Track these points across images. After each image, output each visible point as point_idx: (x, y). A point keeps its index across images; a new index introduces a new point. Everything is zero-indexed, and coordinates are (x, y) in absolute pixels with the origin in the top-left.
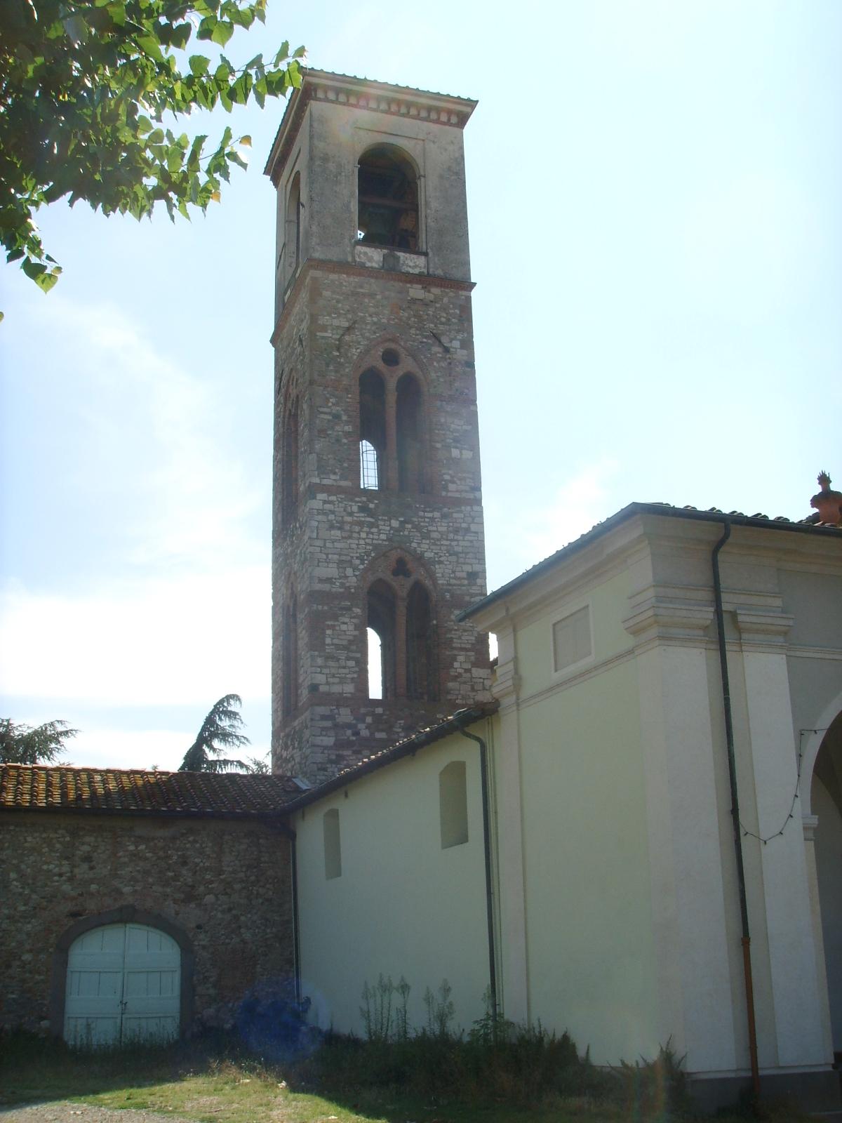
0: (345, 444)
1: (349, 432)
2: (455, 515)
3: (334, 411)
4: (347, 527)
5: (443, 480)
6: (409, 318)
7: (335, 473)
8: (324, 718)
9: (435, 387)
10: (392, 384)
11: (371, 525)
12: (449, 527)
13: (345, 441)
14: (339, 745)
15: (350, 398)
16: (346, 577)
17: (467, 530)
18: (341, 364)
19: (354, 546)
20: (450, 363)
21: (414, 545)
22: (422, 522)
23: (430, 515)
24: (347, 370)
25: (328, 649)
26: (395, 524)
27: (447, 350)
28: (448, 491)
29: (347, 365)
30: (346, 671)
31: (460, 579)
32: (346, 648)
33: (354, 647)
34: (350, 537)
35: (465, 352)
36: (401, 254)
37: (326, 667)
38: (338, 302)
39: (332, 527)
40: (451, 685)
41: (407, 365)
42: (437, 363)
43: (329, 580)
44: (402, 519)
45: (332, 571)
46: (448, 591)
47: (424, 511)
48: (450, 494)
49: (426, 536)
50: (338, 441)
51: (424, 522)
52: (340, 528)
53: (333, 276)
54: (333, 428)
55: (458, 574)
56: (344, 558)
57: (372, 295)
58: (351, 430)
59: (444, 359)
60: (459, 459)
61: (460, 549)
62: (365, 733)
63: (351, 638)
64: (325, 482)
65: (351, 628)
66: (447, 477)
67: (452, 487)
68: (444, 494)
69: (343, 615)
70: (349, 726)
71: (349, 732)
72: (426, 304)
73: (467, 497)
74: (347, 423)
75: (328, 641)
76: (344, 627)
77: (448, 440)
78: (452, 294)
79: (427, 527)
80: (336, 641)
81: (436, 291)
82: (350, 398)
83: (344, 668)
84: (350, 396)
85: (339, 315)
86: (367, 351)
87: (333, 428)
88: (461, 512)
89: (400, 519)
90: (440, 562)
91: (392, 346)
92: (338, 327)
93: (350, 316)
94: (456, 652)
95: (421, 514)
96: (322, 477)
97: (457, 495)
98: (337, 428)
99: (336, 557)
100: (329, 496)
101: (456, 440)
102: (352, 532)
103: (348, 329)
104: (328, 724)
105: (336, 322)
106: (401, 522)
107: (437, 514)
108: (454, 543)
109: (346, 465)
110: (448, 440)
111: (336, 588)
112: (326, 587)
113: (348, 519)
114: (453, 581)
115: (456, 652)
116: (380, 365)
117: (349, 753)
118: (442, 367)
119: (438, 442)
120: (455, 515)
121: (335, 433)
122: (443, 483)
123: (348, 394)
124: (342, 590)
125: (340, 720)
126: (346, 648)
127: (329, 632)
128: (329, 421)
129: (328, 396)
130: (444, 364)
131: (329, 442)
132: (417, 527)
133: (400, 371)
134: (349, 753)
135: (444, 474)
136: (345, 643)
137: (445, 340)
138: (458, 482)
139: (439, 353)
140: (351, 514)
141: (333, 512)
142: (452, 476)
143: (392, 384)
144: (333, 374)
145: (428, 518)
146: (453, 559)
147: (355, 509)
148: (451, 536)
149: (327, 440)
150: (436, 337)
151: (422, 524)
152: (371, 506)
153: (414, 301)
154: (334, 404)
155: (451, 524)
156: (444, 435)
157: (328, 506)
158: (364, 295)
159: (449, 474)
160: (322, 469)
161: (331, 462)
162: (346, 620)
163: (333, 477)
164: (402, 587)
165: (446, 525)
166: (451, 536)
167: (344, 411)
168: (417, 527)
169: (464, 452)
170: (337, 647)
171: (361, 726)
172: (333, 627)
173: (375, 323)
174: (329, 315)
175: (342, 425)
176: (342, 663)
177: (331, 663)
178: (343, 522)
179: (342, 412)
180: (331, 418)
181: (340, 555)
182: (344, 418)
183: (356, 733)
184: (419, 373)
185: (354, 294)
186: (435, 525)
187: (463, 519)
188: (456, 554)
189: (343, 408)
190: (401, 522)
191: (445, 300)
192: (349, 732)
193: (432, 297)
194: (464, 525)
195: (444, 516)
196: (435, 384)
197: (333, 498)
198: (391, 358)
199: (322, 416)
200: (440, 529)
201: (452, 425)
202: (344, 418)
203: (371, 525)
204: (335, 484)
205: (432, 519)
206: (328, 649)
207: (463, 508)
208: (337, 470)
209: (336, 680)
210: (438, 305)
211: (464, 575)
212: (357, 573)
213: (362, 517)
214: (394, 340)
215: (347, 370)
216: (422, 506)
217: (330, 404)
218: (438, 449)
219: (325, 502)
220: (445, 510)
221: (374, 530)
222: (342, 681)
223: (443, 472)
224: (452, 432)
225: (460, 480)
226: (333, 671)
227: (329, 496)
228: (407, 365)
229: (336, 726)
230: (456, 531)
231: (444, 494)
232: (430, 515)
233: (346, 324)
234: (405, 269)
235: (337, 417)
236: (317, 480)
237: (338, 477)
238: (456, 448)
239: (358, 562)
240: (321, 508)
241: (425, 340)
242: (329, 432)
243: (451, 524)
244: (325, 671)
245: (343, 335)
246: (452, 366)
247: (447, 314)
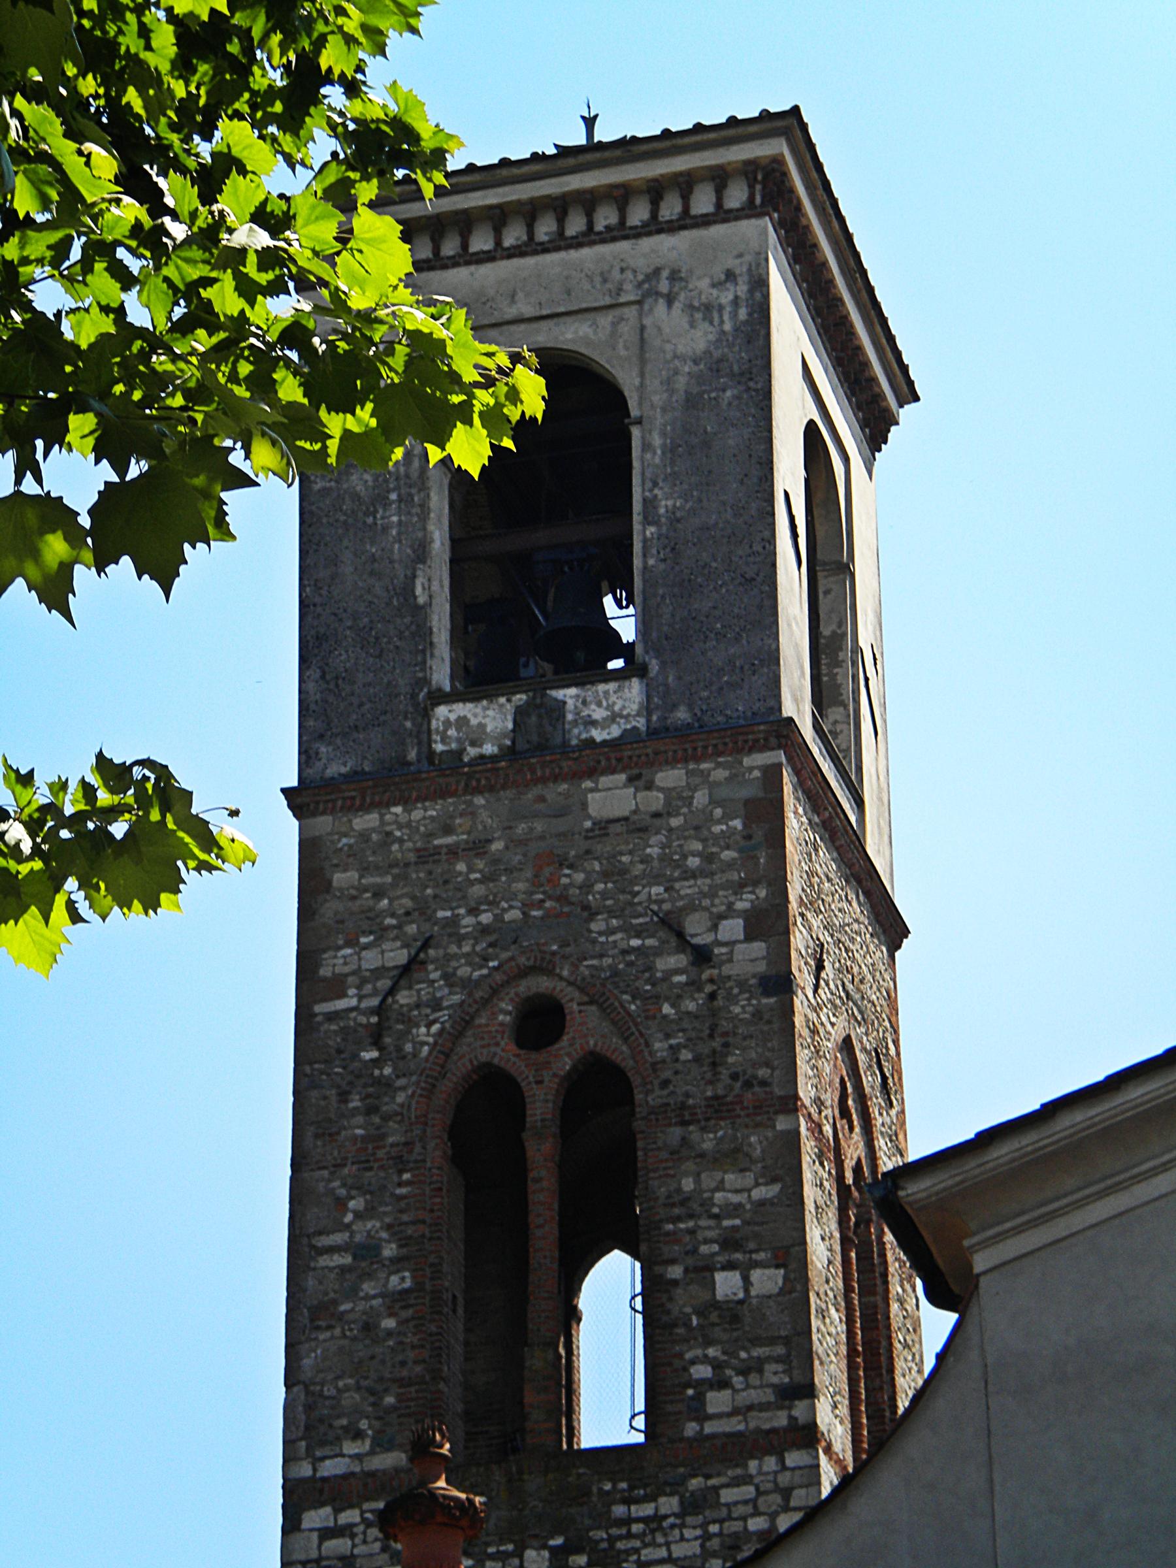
0: (389, 1333)
1: (406, 1291)
2: (727, 1496)
3: (358, 1238)
5: (688, 1385)
6: (587, 887)
7: (358, 1435)
9: (665, 1083)
10: (541, 1105)
12: (706, 1537)
13: (389, 1323)
15: (408, 1183)
18: (386, 1085)
20: (712, 996)
22: (620, 1538)
23: (648, 1510)
24: (401, 1098)
27: (702, 956)
28: (703, 1417)
29: (401, 1082)
35: (758, 948)
36: (568, 695)
38: (378, 894)
41: (587, 1032)
42: (673, 1006)
44: (558, 1541)
47: (628, 1501)
48: (709, 1428)
50: (369, 1327)
51: (630, 1536)
53: (367, 821)
54: (352, 1293)
57: (478, 847)
58: (408, 1284)
59: (694, 985)
60: (741, 1302)
64: (329, 1468)
66: (702, 1371)
67: (717, 1401)
68: (691, 1429)
72: (636, 827)
73: (767, 1426)
74: (397, 1263)
77: (704, 1249)
78: (720, 774)
79: (637, 1551)
81: (671, 777)
82: (408, 1183)
84: (406, 1176)
85: (381, 933)
86: (463, 1023)
87: (352, 1293)
88: (746, 1480)
89: (552, 1543)
91: (542, 984)
92: (378, 972)
93: (412, 929)
95: (619, 1510)
96: (318, 1454)
97: (735, 1425)
98: (368, 1287)
100: (337, 1511)
101: (730, 1242)
103: (406, 970)
105: (371, 960)
106: (554, 1551)
107: (669, 1504)
109: (390, 1400)
110: (704, 1249)
116: (505, 1053)
118: (688, 1013)
119: (673, 1261)
121: (361, 1306)
122: (690, 1392)
123: (400, 1172)
128: (343, 1270)
129: (343, 1192)
131: (344, 1336)
133: (563, 1058)
135: (693, 1362)
137: (697, 928)
138: (738, 1381)
139: (678, 972)
142: (717, 1366)
143: (541, 1105)
144: (360, 1120)
145: (638, 1520)
149: (337, 1332)
150: (671, 926)
151: (620, 1545)
153: (603, 827)
154: (358, 1215)
155: (714, 1528)
156: (692, 1232)
158: (453, 852)
159: (706, 1360)
161: (352, 1399)
163: (350, 1448)
165: (698, 1532)
167: (389, 1227)
169: (756, 1275)
173: (485, 930)
174: (351, 942)
175: (382, 1275)
179: (384, 1235)
180: (347, 1260)
184: (619, 1051)
185: (426, 856)
186: (660, 1539)
187: (754, 1501)
189: (387, 1220)
190: (554, 1551)
191: (701, 798)
193: (656, 800)
195: (693, 1506)
196: (667, 1074)
197: (350, 1516)
198: (540, 1023)
199: (324, 1261)
200: (678, 1551)
201: (718, 1195)
202: (389, 1251)
204: (358, 1469)
207: (753, 1465)
208: (364, 1424)
210: (675, 822)
214: (544, 967)
215: (401, 1098)
216: (623, 1485)
217: (349, 1218)
218: (675, 1283)
219: (326, 1534)
220: (695, 1483)
223: (688, 1356)
224: (716, 1217)
225: (744, 1372)
227: (337, 1511)
228: (587, 1032)
231: (691, 1429)
232: (648, 1510)
233: (400, 957)
234: (577, 734)
235: (366, 1252)
238: (730, 1266)
240: (314, 1554)
241: (635, 942)
242: (343, 1307)
243: (714, 1528)
245: (392, 992)
246: (720, 1002)
247: (704, 841)
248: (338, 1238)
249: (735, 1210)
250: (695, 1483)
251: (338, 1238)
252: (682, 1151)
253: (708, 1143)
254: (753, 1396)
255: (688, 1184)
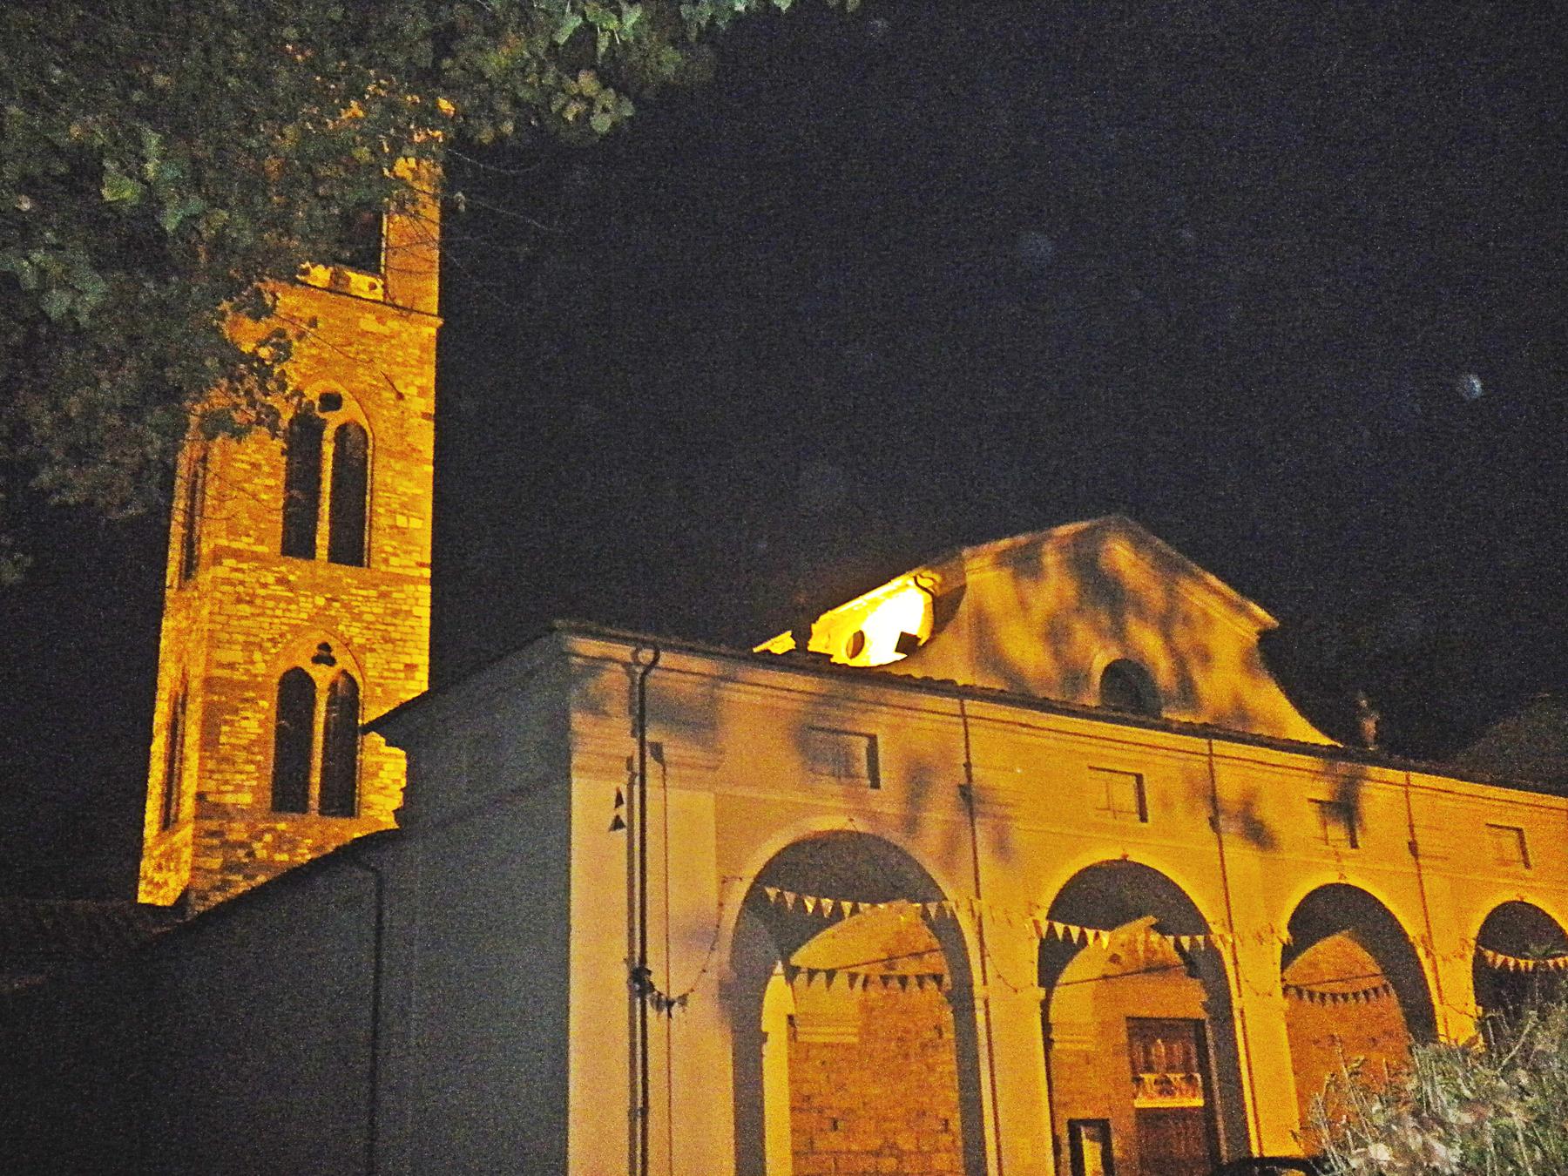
4: (258, 601)
7: (248, 536)
8: (212, 834)
11: (289, 601)
14: (228, 867)
16: (252, 662)
17: (409, 613)
19: (266, 626)
21: (341, 628)
25: (224, 750)
26: (321, 601)
27: (400, 396)
30: (244, 777)
31: (394, 671)
32: (246, 748)
33: (256, 750)
34: (262, 614)
37: (221, 772)
39: (239, 601)
40: (372, 798)
41: (351, 410)
43: (231, 666)
45: (236, 655)
46: (379, 685)
48: (391, 570)
49: (357, 617)
52: (250, 603)
55: (394, 666)
56: (252, 639)
59: (397, 406)
61: (398, 636)
62: (261, 854)
63: (253, 737)
64: (235, 545)
65: (256, 724)
67: (393, 561)
69: (244, 709)
70: (242, 845)
71: (241, 853)
72: (380, 339)
74: (270, 475)
75: (223, 739)
76: (244, 723)
80: (233, 740)
83: (241, 773)
90: (372, 650)
94: (381, 759)
95: (354, 591)
97: (400, 571)
98: (256, 480)
99: (241, 638)
101: (403, 505)
102: (264, 608)
104: (216, 842)
107: (373, 593)
108: (391, 628)
111: (238, 676)
112: (225, 673)
113: (262, 592)
114: (386, 674)
115: (381, 759)
117: (240, 878)
120: (395, 595)
124: (245, 678)
125: (232, 837)
126: (246, 748)
127: (225, 728)
130: (395, 413)
132: (347, 606)
134: (240, 878)
136: (244, 742)
140: (265, 586)
141: (242, 583)
146: (389, 646)
147: (271, 579)
148: (389, 619)
152: (292, 578)
153: (365, 334)
157: (239, 576)
160: (233, 532)
162: (248, 714)
163: (245, 539)
164: (322, 676)
166: (389, 619)
168: (347, 606)
170: (233, 746)
171: (257, 845)
172: (230, 723)
176: (241, 767)
177: (224, 766)
178: (254, 595)
181: (248, 634)
182: (266, 469)
183: (251, 854)
184: (364, 423)
188: (392, 641)
192: (241, 853)
194: (405, 608)
195: (383, 595)
197: (244, 566)
199: (239, 465)
200: (375, 610)
202: (266, 469)
203: (289, 601)
205: (367, 598)
206: (224, 750)
209: (230, 788)
211: (401, 667)
212: (268, 658)
213: (280, 591)
221: (293, 607)
222: (239, 789)
226: (228, 777)
228: (351, 410)
229: (225, 843)
230: (395, 614)
231: (383, 568)
235: (255, 466)
236: (224, 542)
237: (251, 540)
239: (269, 645)
244: (216, 776)
248: (244, 458)
249: (404, 494)
250: (384, 588)
251: (244, 458)
252: (387, 467)
253: (398, 467)
254: (405, 562)
255: (389, 480)
